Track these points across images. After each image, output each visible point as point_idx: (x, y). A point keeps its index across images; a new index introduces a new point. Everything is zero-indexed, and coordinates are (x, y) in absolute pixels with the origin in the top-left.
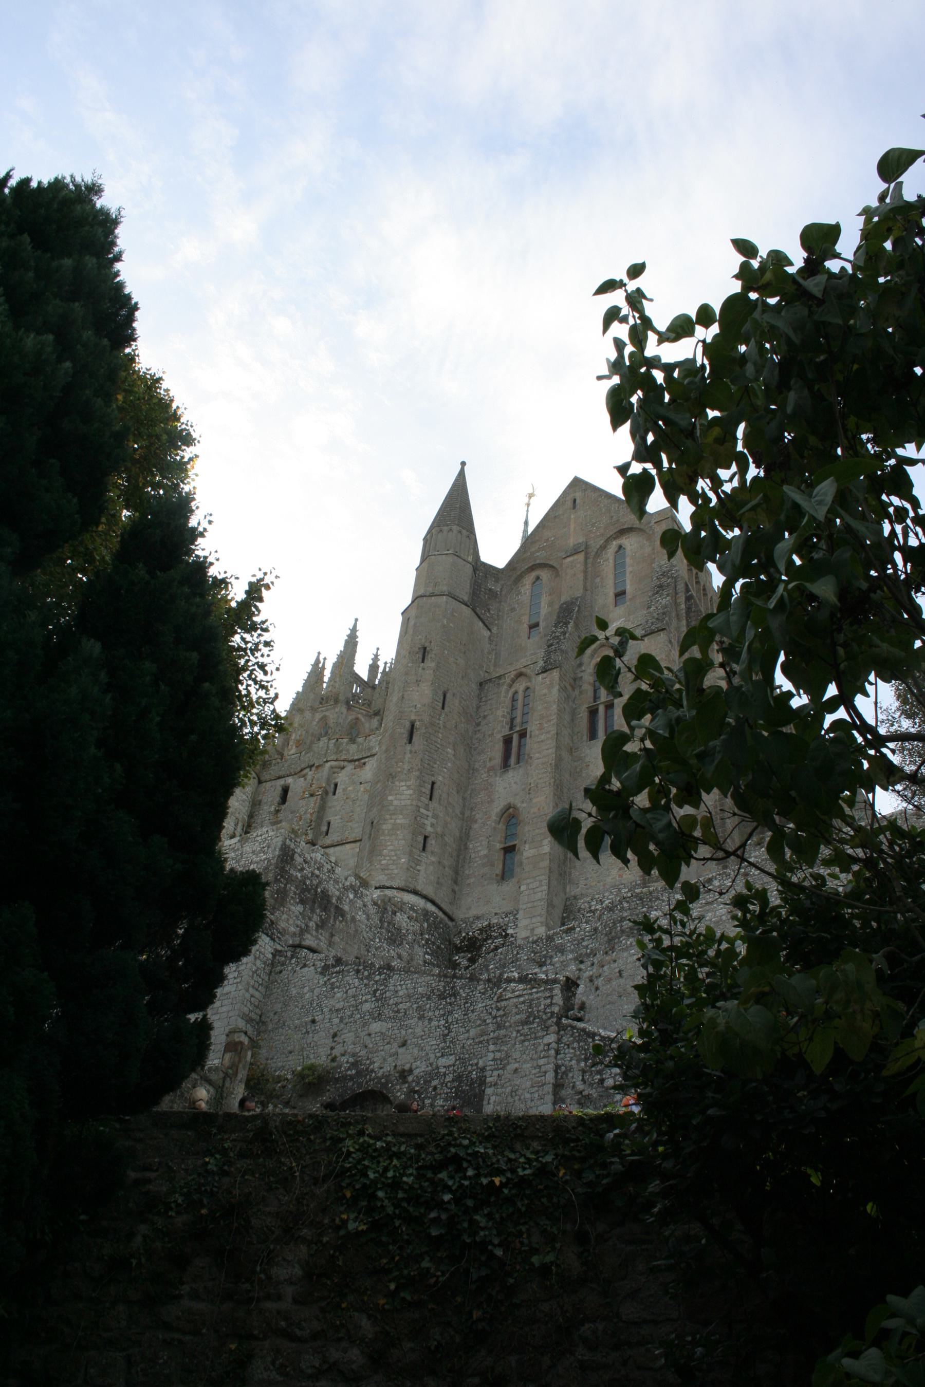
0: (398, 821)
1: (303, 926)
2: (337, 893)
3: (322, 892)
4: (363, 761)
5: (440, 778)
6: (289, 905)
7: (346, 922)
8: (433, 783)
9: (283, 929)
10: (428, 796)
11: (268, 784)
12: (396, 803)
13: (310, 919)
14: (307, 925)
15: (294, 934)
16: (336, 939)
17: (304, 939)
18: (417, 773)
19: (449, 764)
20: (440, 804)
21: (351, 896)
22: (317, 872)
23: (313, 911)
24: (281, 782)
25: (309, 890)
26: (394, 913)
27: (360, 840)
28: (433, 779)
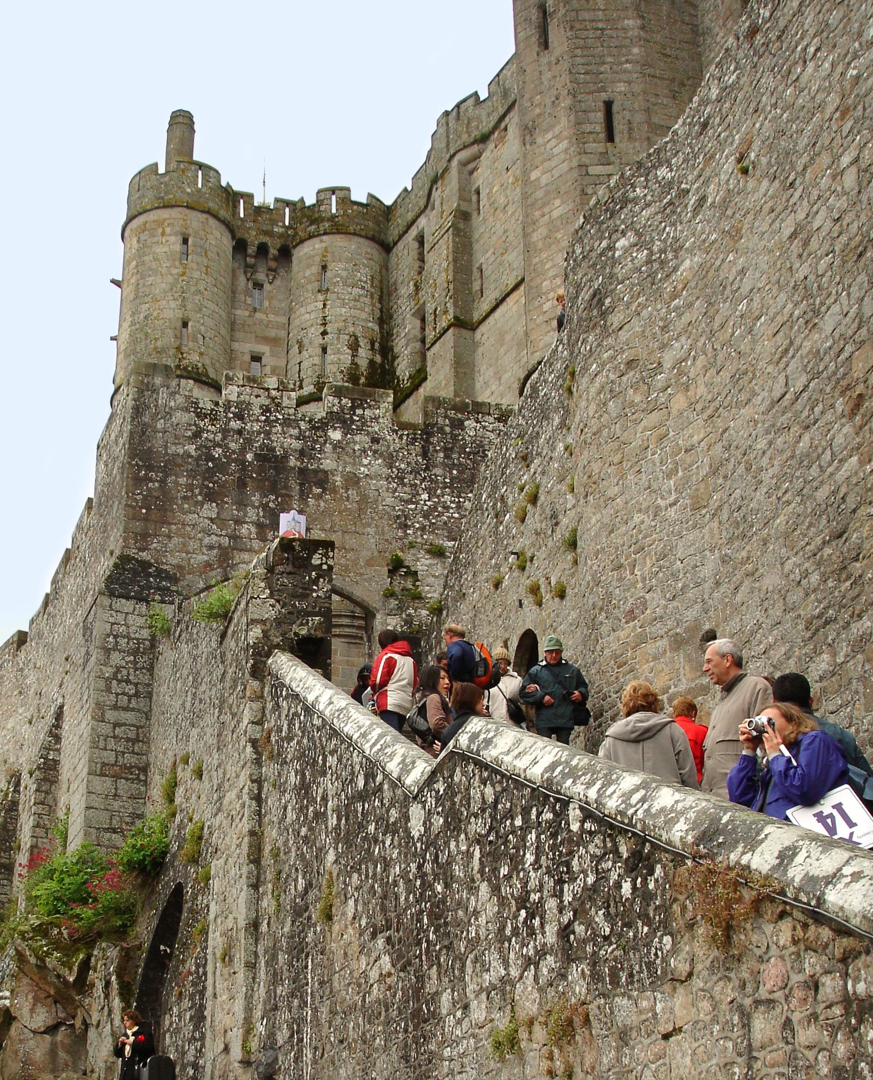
0: (555, 214)
2: (297, 445)
3: (256, 455)
4: (503, 125)
5: (622, 87)
7: (334, 491)
8: (608, 105)
10: (602, 136)
11: (400, 245)
12: (544, 180)
13: (238, 522)
14: (234, 537)
15: (208, 565)
18: (566, 102)
19: (636, 50)
20: (630, 138)
21: (336, 435)
22: (235, 425)
23: (242, 504)
24: (413, 232)
26: (458, 425)
27: (523, 280)
28: (604, 96)
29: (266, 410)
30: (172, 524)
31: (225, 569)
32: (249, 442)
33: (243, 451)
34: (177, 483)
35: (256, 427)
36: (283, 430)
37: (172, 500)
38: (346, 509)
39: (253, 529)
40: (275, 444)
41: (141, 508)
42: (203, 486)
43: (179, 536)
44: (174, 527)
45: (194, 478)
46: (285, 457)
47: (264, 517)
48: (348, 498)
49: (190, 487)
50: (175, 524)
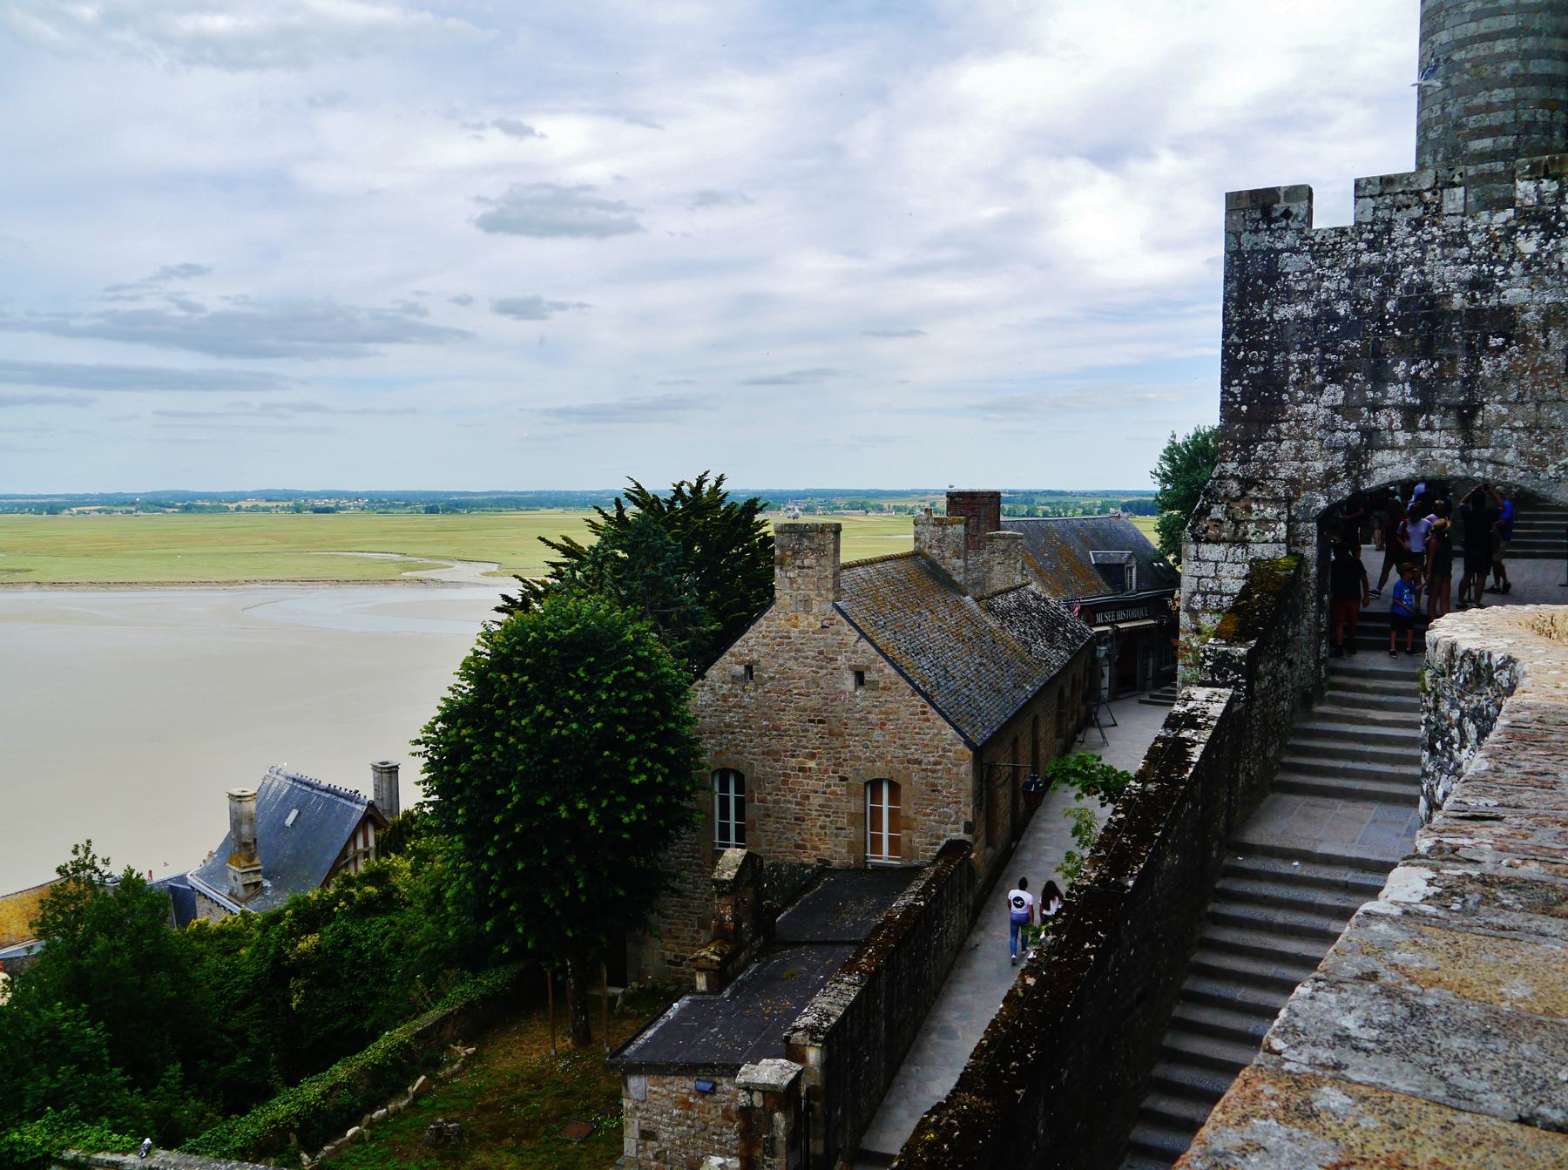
1: (1355, 438)
2: (1467, 273)
3: (1402, 304)
6: (1292, 410)
7: (1524, 339)
9: (1291, 481)
13: (1375, 407)
15: (1330, 476)
16: (1494, 408)
17: (1368, 474)
21: (1528, 246)
23: (1380, 377)
25: (1349, 329)
29: (1418, 224)
30: (1282, 421)
31: (1356, 481)
32: (1389, 282)
33: (1382, 299)
34: (1287, 363)
35: (1401, 257)
36: (1442, 252)
37: (1281, 386)
38: (1544, 364)
39: (1397, 418)
40: (1429, 278)
41: (1241, 404)
42: (1322, 362)
43: (1291, 438)
44: (1283, 426)
45: (1309, 350)
46: (1448, 296)
47: (1412, 395)
48: (1547, 344)
49: (1304, 366)
50: (1287, 421)
